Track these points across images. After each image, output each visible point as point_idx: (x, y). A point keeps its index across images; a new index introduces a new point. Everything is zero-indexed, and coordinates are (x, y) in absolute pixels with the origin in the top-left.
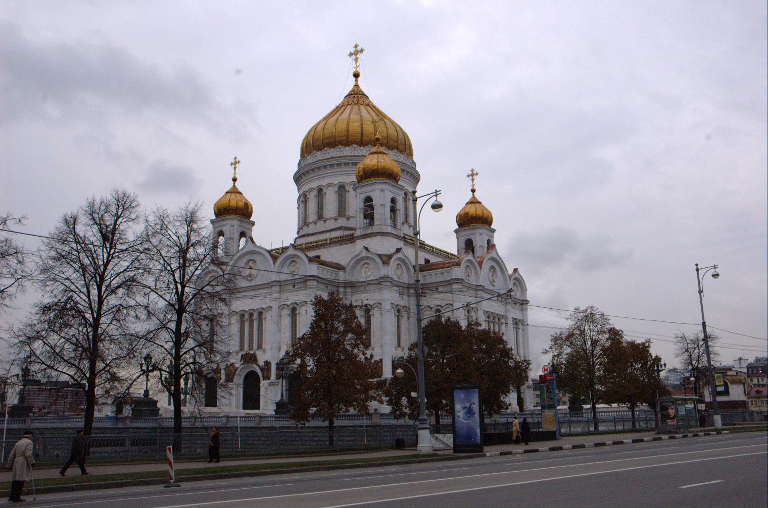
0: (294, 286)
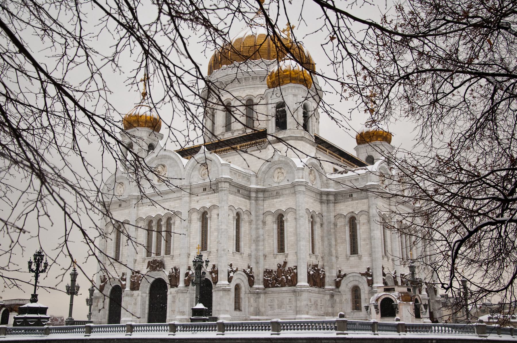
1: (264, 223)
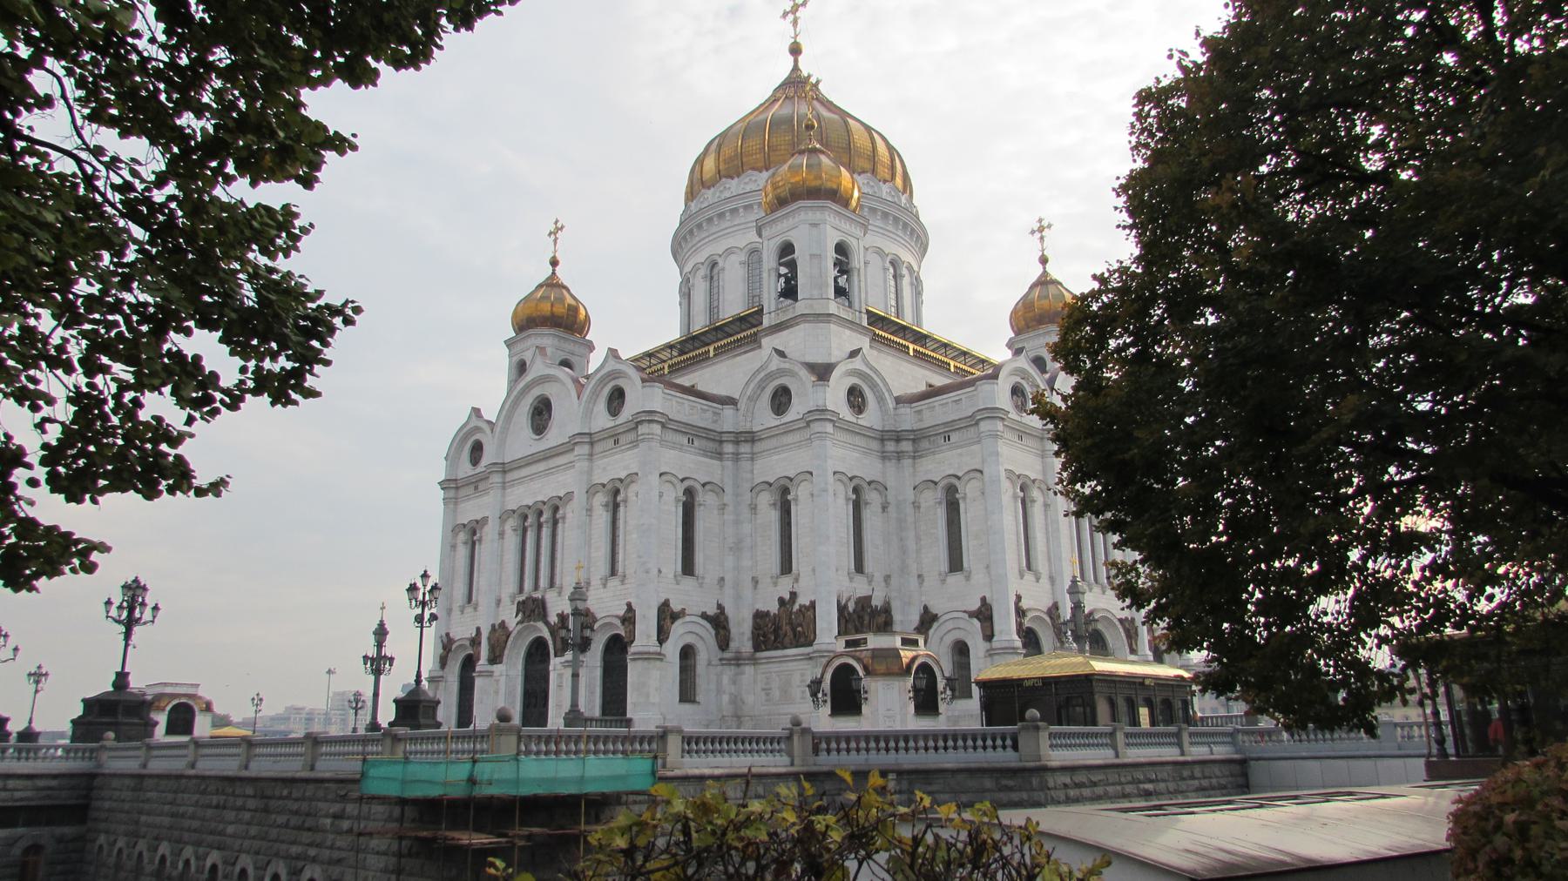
0: (616, 442)
1: (754, 508)
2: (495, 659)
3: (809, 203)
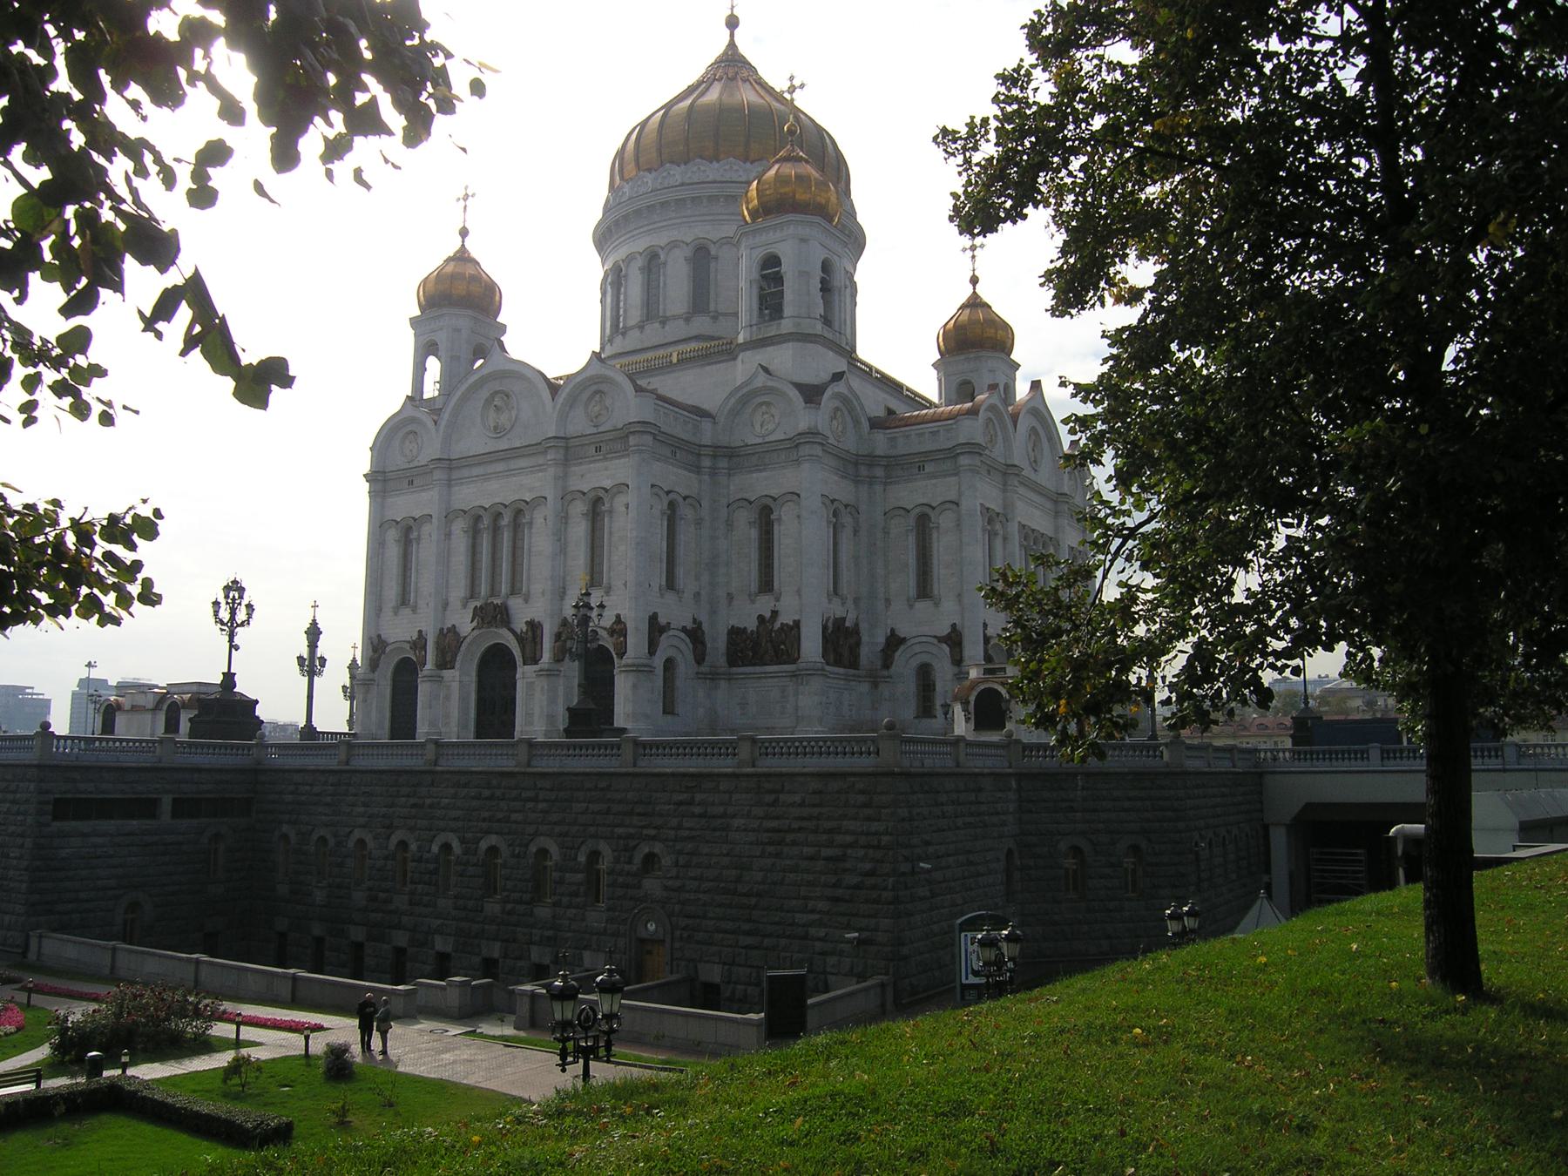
0: (598, 449)
1: (730, 525)
2: (445, 662)
3: (799, 217)
